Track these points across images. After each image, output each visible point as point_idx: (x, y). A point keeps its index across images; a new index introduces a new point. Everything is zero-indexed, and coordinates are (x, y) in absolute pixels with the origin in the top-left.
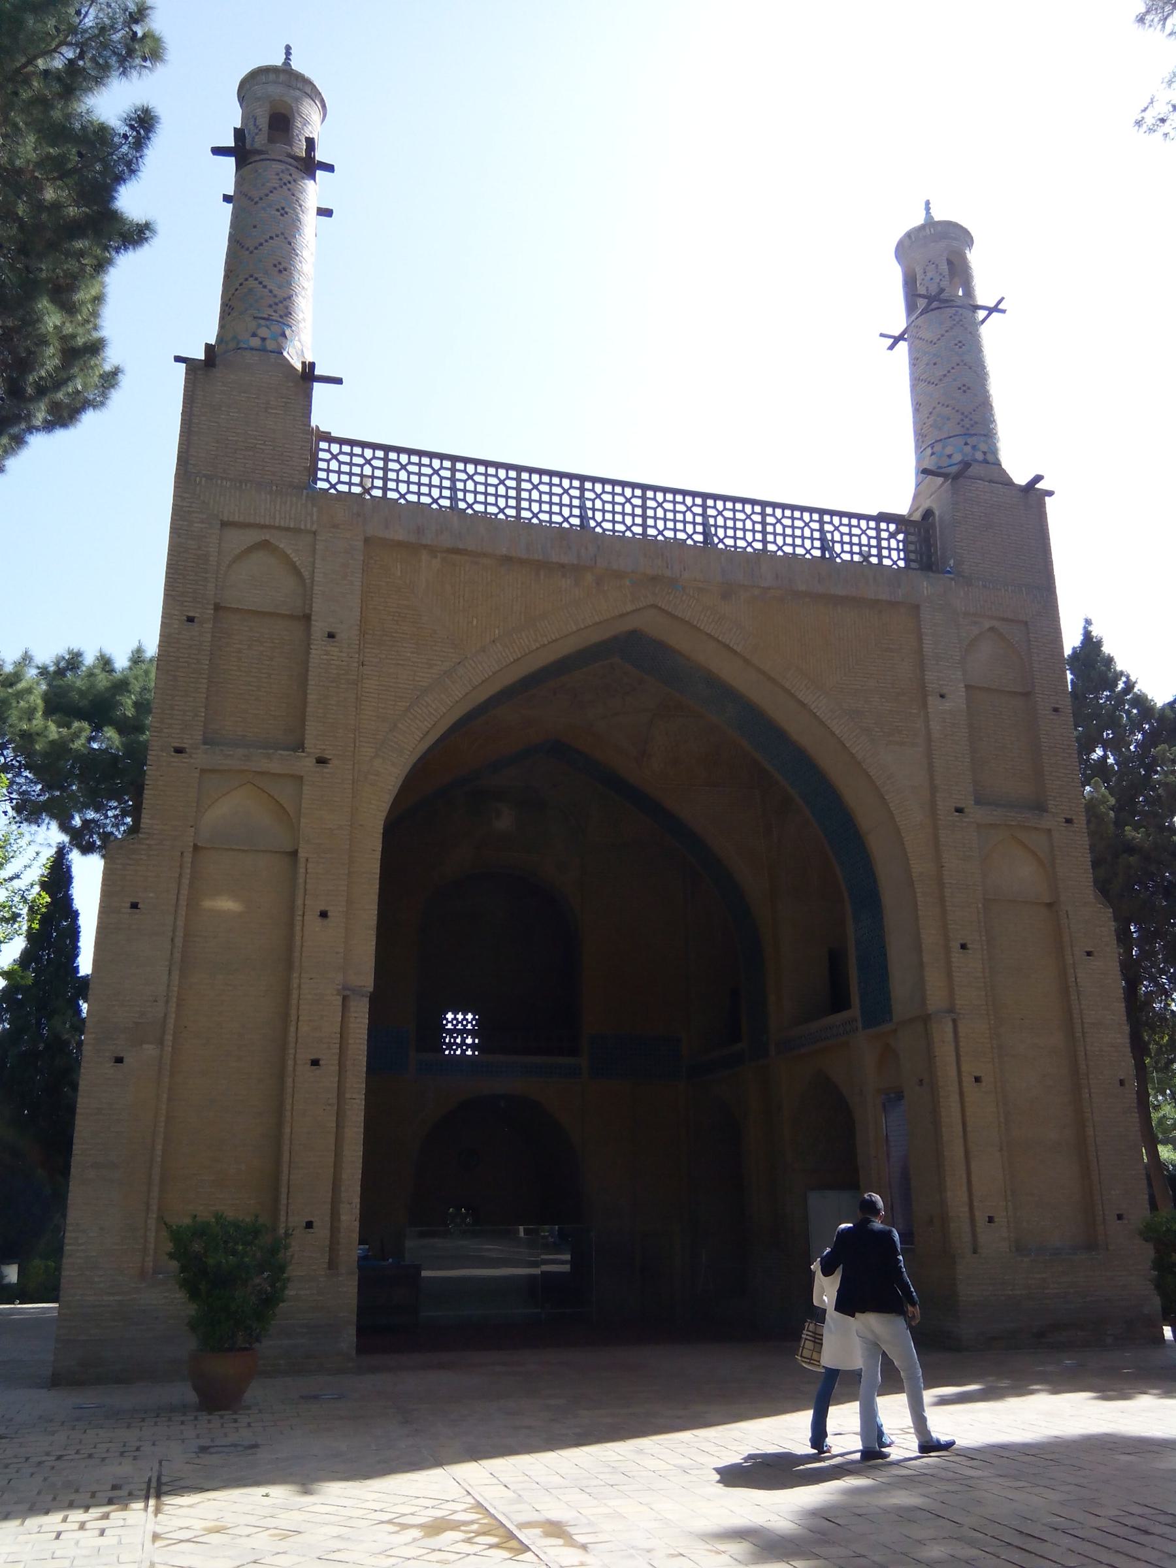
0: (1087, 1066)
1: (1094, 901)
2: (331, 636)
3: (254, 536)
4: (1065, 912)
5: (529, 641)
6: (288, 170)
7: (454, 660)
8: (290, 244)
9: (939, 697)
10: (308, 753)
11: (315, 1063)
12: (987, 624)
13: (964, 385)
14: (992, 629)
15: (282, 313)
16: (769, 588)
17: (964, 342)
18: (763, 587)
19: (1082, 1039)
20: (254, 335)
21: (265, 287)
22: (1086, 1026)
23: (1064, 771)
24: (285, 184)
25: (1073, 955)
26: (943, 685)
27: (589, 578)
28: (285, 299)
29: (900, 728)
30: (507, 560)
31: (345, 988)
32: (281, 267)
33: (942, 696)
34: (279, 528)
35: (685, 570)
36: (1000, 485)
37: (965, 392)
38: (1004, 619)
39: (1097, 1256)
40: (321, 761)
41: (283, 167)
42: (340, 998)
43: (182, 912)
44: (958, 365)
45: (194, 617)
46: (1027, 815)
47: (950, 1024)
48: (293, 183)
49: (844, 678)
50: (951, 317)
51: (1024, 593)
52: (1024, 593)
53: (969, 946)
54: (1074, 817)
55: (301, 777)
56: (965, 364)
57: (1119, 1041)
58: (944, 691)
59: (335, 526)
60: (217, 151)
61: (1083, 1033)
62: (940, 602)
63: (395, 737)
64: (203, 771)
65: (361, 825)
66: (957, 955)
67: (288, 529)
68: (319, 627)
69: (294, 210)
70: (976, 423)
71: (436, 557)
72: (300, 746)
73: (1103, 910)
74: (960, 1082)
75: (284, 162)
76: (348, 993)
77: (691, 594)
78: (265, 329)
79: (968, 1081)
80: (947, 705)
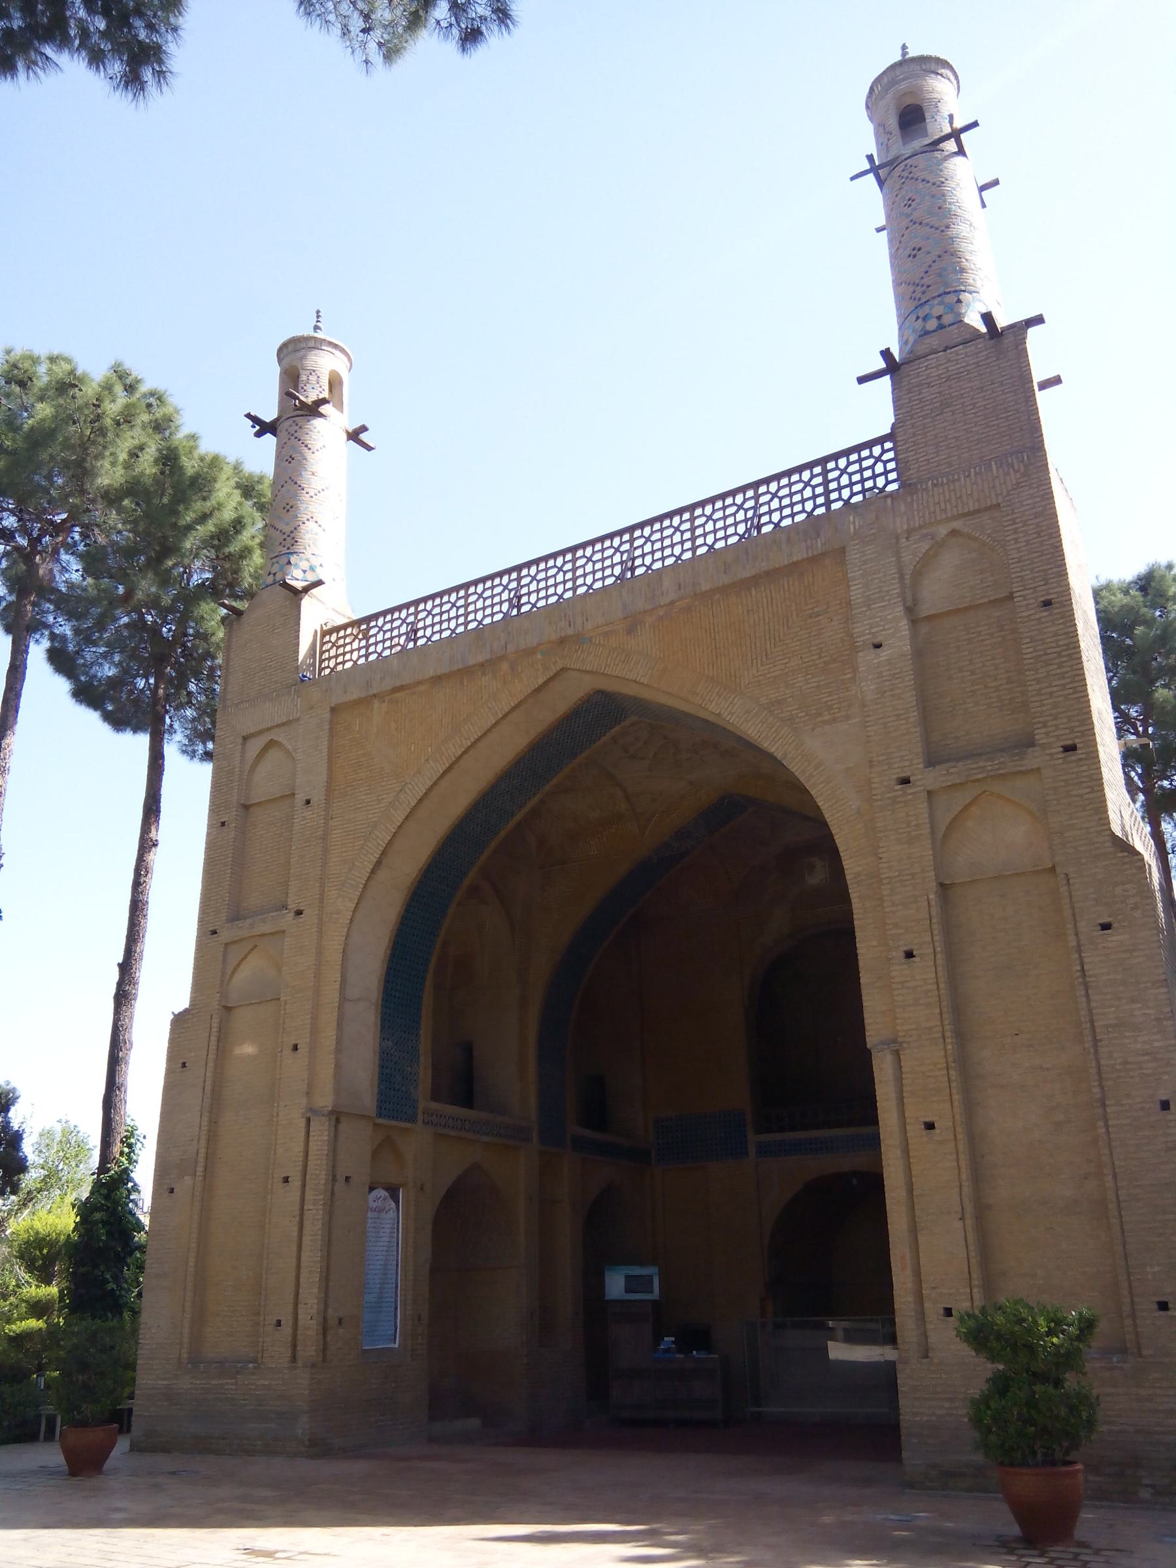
0: (1101, 1086)
1: (1113, 849)
2: (308, 802)
4: (1063, 876)
5: (455, 749)
6: (294, 422)
7: (397, 789)
8: (296, 483)
9: (873, 651)
10: (290, 909)
11: (286, 1180)
12: (943, 531)
13: (914, 249)
14: (953, 533)
15: (289, 545)
16: (672, 603)
17: (913, 198)
18: (665, 605)
19: (1092, 1050)
20: (270, 574)
21: (277, 530)
22: (1098, 1030)
23: (1060, 682)
24: (292, 435)
25: (1077, 935)
26: (877, 632)
27: (505, 666)
28: (292, 532)
29: (829, 703)
30: (437, 680)
31: (311, 1110)
32: (288, 507)
33: (878, 646)
34: (278, 726)
35: (587, 620)
36: (961, 347)
37: (915, 256)
38: (964, 515)
39: (1119, 1365)
40: (299, 913)
41: (290, 422)
42: (303, 1121)
43: (211, 1065)
44: (907, 228)
45: (225, 822)
46: (1002, 759)
47: (890, 1057)
48: (300, 430)
49: (762, 668)
50: (899, 176)
51: (994, 467)
52: (994, 467)
53: (915, 953)
54: (1077, 741)
55: (284, 932)
56: (915, 223)
57: (1157, 1044)
58: (877, 641)
59: (312, 708)
60: (258, 434)
61: (1096, 1041)
62: (872, 532)
63: (353, 875)
64: (227, 944)
65: (327, 961)
66: (898, 968)
67: (283, 724)
68: (300, 797)
69: (301, 453)
70: (928, 286)
71: (384, 702)
72: (285, 907)
73: (1127, 860)
74: (904, 1131)
75: (293, 417)
76: (309, 1115)
77: (597, 642)
78: (276, 565)
79: (915, 1130)
80: (884, 654)
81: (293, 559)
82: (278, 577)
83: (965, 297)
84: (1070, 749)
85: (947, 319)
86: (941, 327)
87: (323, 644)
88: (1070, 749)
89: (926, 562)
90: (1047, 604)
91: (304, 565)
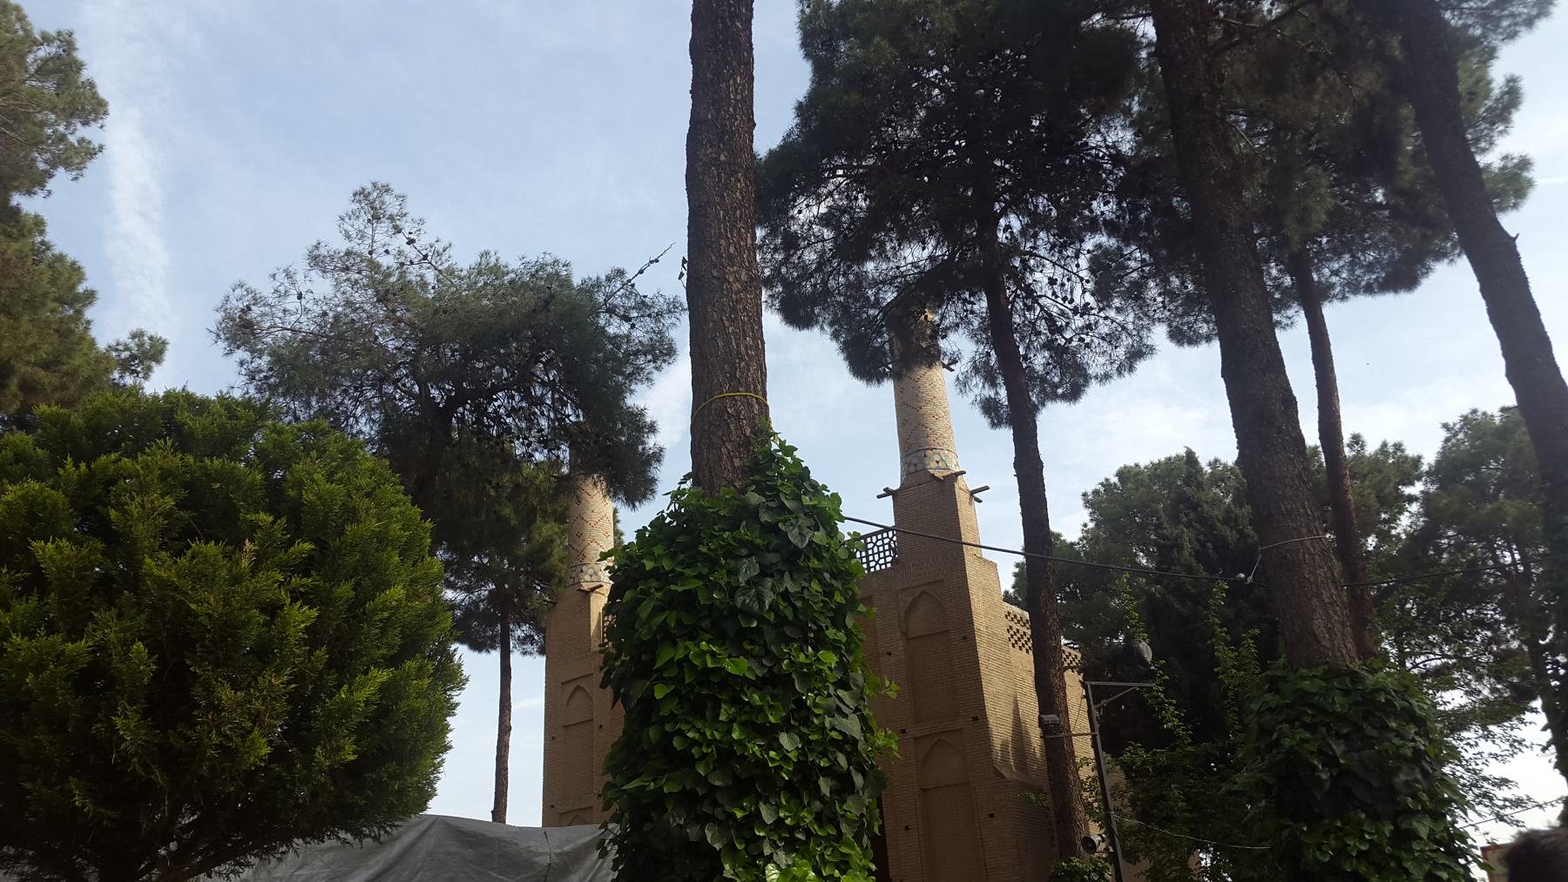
2: (601, 726)
3: (571, 687)
14: (924, 592)
33: (890, 654)
55: (591, 808)
64: (561, 814)
68: (596, 723)
80: (892, 659)
81: (584, 568)
82: (576, 580)
83: (929, 453)
84: (976, 719)
85: (919, 467)
86: (917, 471)
87: (604, 622)
88: (976, 719)
89: (910, 610)
90: (965, 638)
91: (591, 571)
